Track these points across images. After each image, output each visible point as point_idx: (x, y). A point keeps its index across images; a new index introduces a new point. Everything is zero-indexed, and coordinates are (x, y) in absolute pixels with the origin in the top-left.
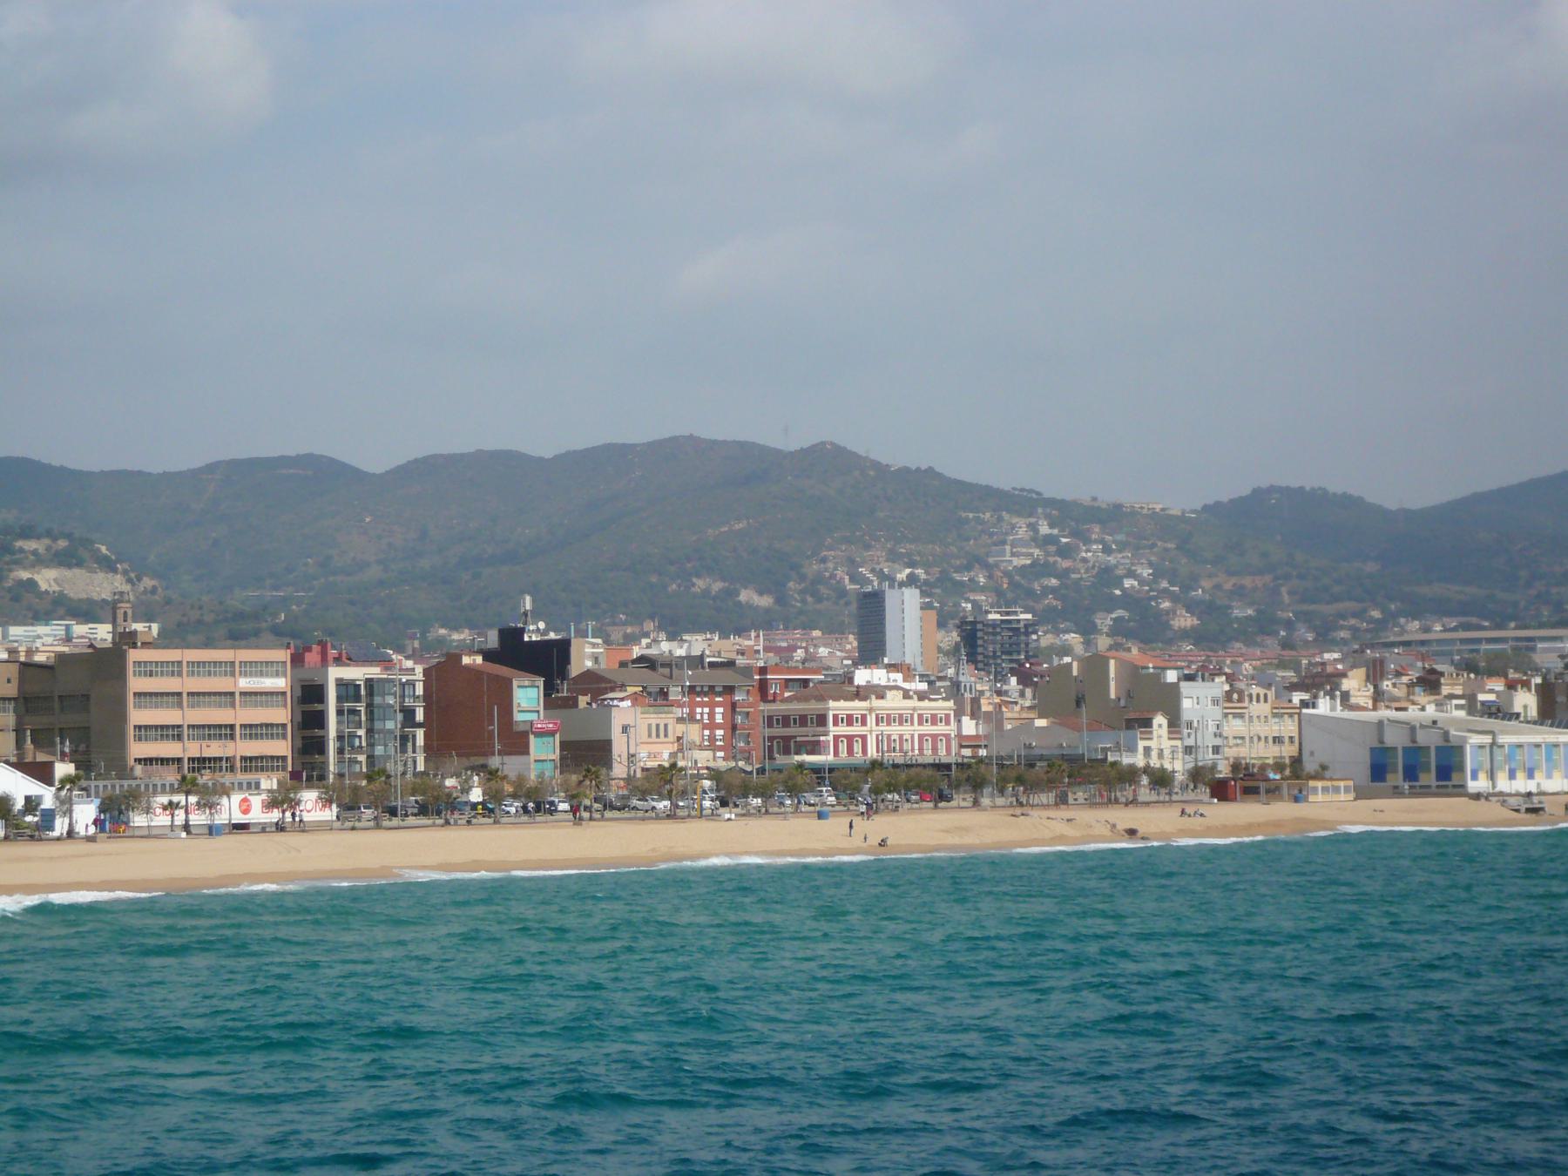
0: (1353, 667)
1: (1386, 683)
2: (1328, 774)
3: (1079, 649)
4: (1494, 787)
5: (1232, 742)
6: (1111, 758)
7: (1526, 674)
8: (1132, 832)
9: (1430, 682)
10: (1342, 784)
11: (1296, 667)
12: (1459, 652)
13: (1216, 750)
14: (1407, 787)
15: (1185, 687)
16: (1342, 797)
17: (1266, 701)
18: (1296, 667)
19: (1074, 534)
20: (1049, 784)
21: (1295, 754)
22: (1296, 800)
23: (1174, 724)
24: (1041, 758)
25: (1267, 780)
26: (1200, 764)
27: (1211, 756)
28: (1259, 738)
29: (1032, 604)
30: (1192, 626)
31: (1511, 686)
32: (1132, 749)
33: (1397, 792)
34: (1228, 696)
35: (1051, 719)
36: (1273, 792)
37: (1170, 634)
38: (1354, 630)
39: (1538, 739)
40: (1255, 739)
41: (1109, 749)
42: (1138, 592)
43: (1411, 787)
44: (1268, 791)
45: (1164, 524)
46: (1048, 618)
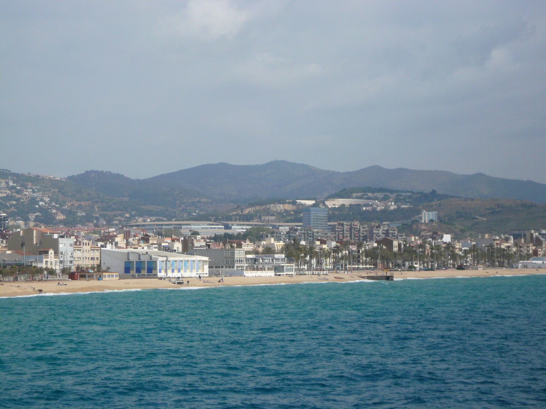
0: (119, 234)
2: (110, 270)
3: (23, 226)
4: (167, 275)
5: (76, 259)
6: (33, 265)
7: (178, 236)
8: (40, 291)
9: (146, 239)
10: (115, 274)
11: (100, 233)
13: (71, 262)
14: (137, 275)
15: (61, 240)
16: (115, 278)
17: (89, 245)
18: (100, 233)
19: (21, 186)
20: (12, 273)
21: (99, 263)
22: (99, 279)
23: (56, 253)
24: (9, 264)
25: (89, 272)
26: (65, 267)
27: (69, 264)
28: (86, 258)
29: (6, 210)
30: (63, 219)
31: (173, 241)
32: (41, 262)
33: (133, 277)
34: (76, 243)
35: (12, 251)
36: (91, 277)
37: (55, 221)
38: (120, 221)
39: (182, 259)
40: (85, 258)
41: (33, 261)
42: (44, 206)
44: (89, 276)
45: (54, 183)
46: (12, 215)
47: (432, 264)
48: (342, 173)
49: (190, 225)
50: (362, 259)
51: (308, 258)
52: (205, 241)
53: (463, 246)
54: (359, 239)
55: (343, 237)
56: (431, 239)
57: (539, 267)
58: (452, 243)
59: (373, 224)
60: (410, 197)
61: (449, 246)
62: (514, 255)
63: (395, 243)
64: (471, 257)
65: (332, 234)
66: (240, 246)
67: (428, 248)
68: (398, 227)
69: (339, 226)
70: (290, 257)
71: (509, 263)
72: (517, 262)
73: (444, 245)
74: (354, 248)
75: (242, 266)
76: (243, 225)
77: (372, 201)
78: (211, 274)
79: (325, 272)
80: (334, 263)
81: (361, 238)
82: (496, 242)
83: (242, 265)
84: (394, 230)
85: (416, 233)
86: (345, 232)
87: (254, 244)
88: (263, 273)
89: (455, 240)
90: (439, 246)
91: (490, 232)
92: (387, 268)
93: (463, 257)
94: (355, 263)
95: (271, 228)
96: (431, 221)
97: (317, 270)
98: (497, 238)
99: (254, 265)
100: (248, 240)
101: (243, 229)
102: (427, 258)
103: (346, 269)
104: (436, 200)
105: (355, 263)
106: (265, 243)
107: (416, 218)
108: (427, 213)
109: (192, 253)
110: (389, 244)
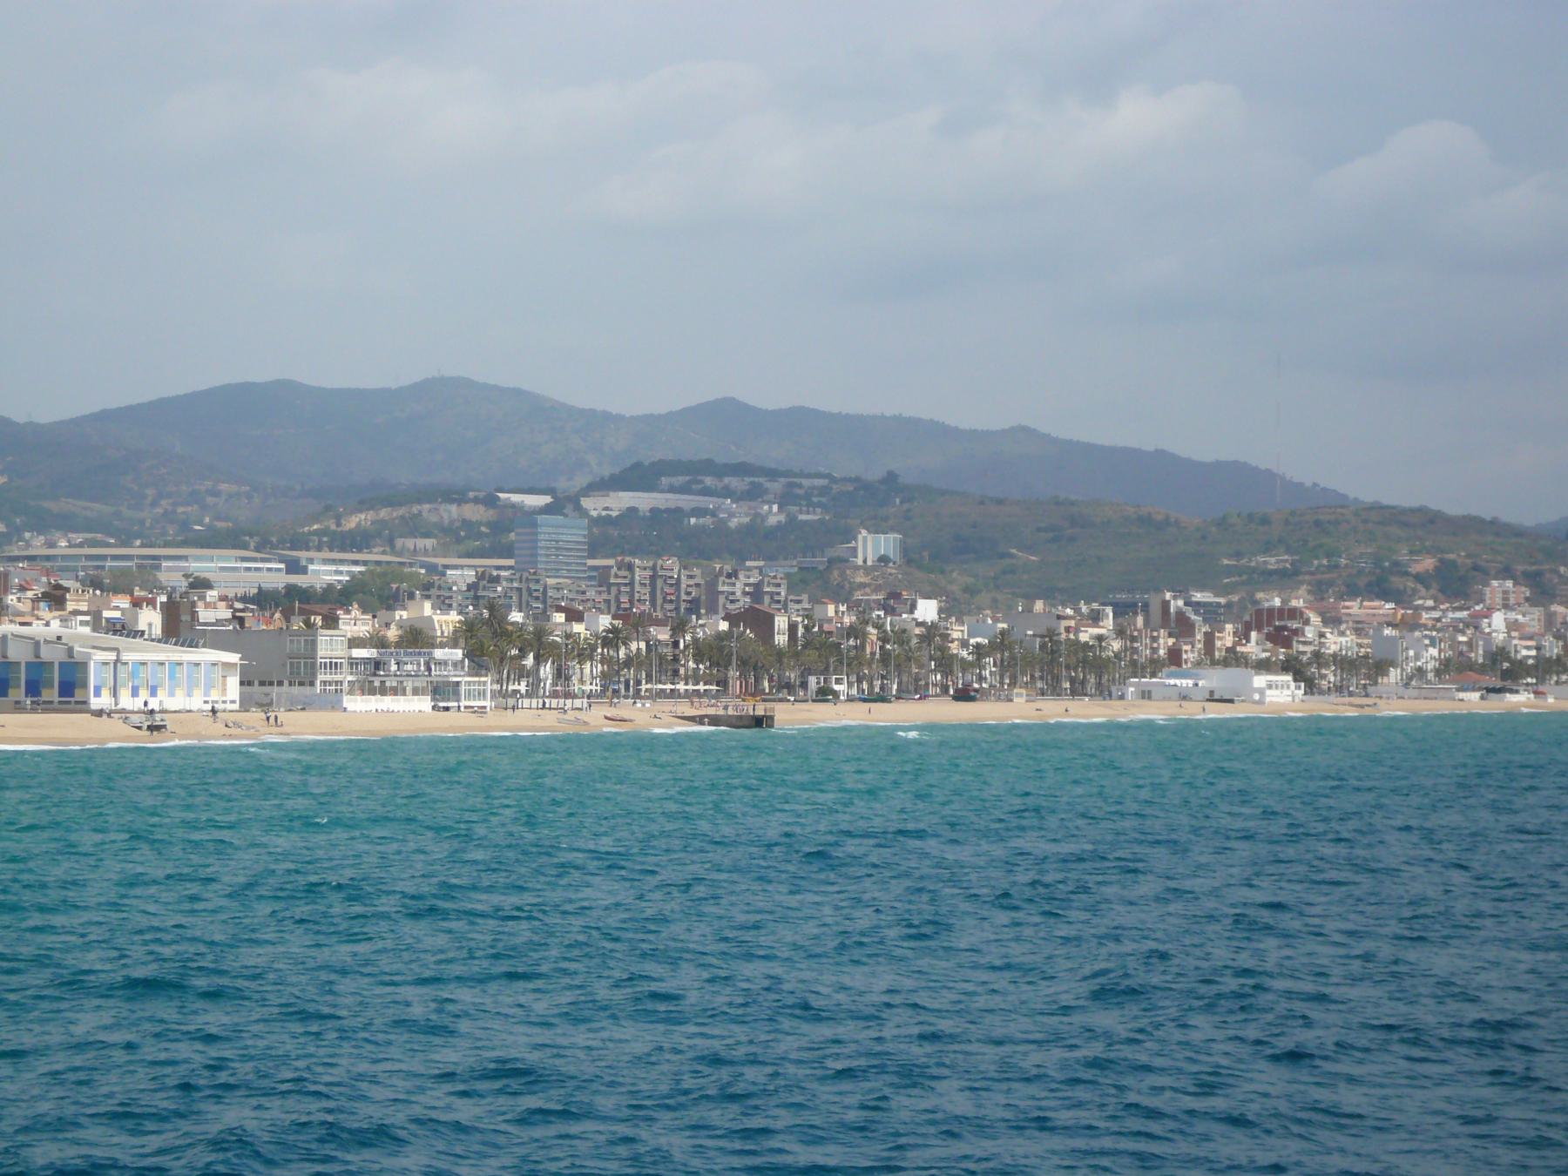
1: (10, 597)
4: (116, 704)
7: (151, 592)
9: (55, 598)
12: (84, 568)
14: (28, 702)
31: (137, 603)
39: (161, 657)
43: (32, 702)
47: (882, 683)
48: (632, 417)
49: (185, 558)
50: (684, 666)
51: (529, 661)
52: (231, 607)
53: (971, 635)
54: (677, 609)
55: (631, 602)
56: (882, 613)
57: (1185, 698)
58: (942, 624)
59: (718, 567)
60: (824, 491)
61: (932, 632)
62: (1114, 663)
63: (781, 622)
64: (995, 665)
65: (600, 593)
66: (331, 622)
67: (874, 638)
68: (788, 576)
69: (619, 569)
70: (478, 659)
71: (1099, 685)
72: (1123, 681)
73: (917, 631)
74: (663, 635)
75: (336, 682)
76: (342, 562)
77: (715, 499)
78: (246, 703)
79: (578, 703)
80: (604, 675)
81: (683, 606)
82: (1064, 623)
83: (338, 677)
84: (779, 585)
85: (840, 594)
86: (637, 588)
87: (374, 617)
88: (398, 701)
89: (949, 616)
90: (904, 631)
91: (1049, 594)
92: (757, 692)
93: (971, 665)
94: (663, 678)
95: (423, 571)
96: (883, 560)
97: (555, 695)
98: (1069, 611)
99: (372, 678)
100: (356, 606)
101: (341, 573)
102: (870, 665)
103: (637, 695)
104: (898, 501)
105: (663, 678)
106: (405, 614)
107: (839, 550)
108: (870, 537)
109: (192, 641)
110: (763, 623)
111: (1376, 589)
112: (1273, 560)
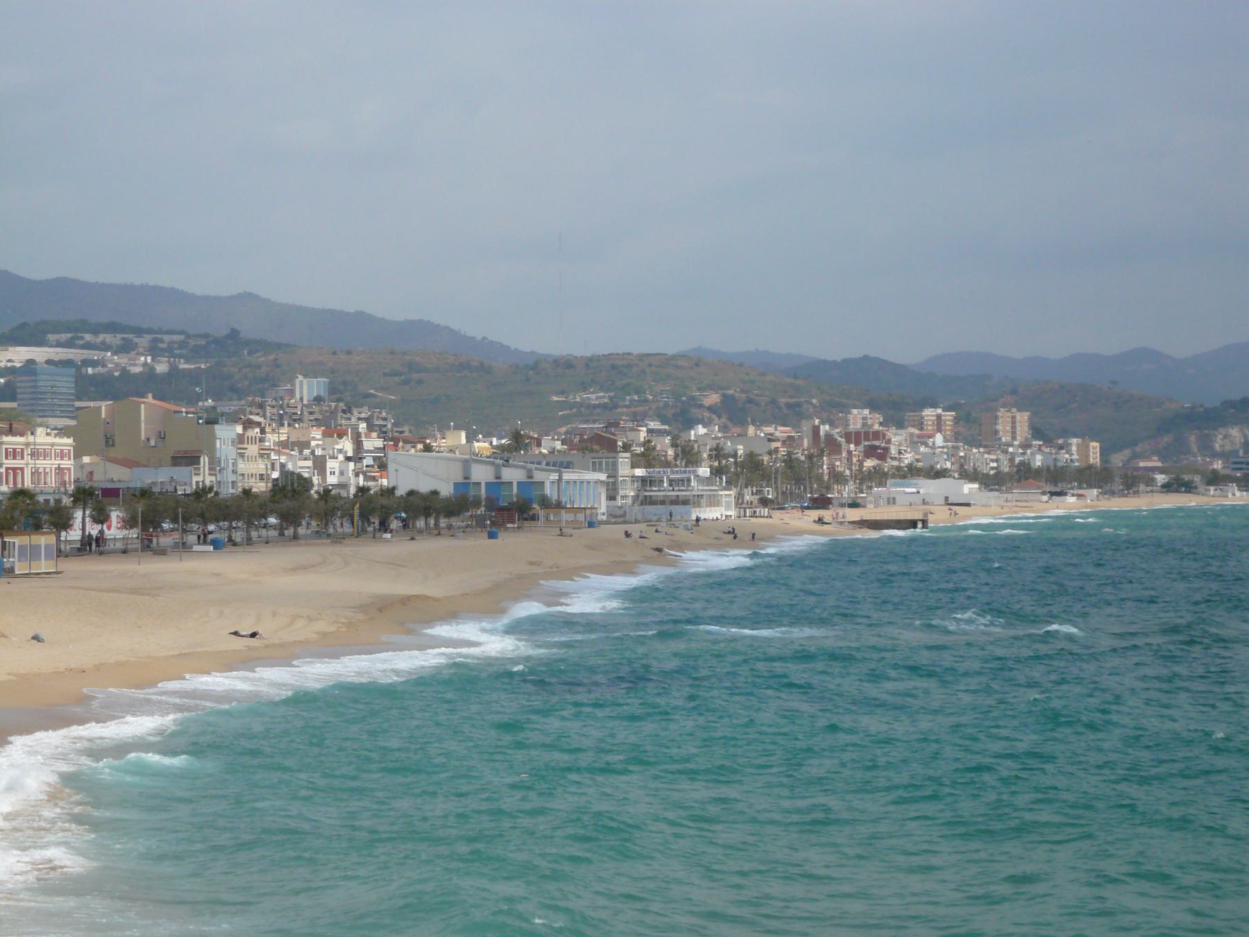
77: (97, 352)
111: (681, 419)
112: (593, 396)
